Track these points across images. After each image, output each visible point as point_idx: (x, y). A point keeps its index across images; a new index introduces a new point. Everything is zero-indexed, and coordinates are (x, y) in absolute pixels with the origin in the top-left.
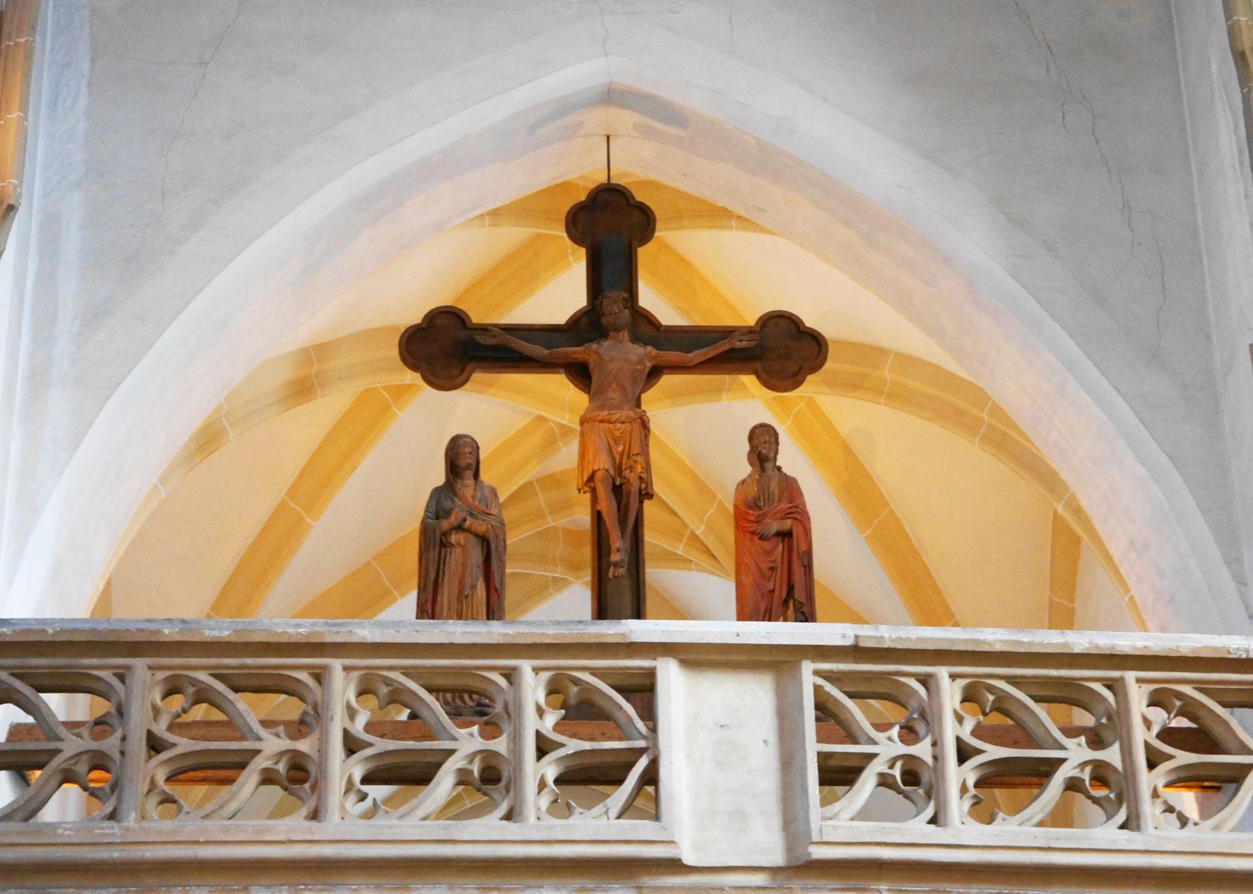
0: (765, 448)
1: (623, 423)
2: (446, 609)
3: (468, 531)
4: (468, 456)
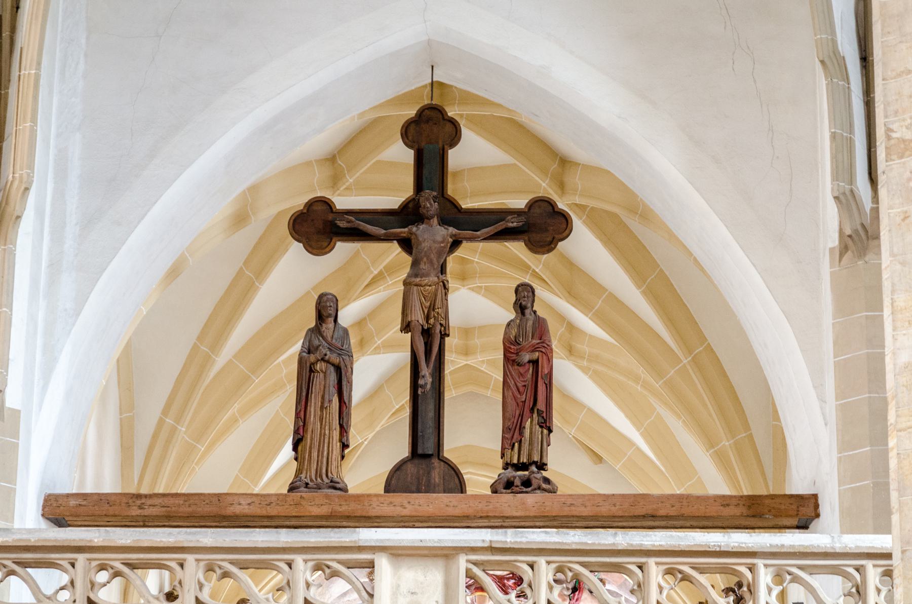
0: (524, 301)
1: (430, 286)
2: (312, 416)
3: (328, 362)
4: (329, 308)
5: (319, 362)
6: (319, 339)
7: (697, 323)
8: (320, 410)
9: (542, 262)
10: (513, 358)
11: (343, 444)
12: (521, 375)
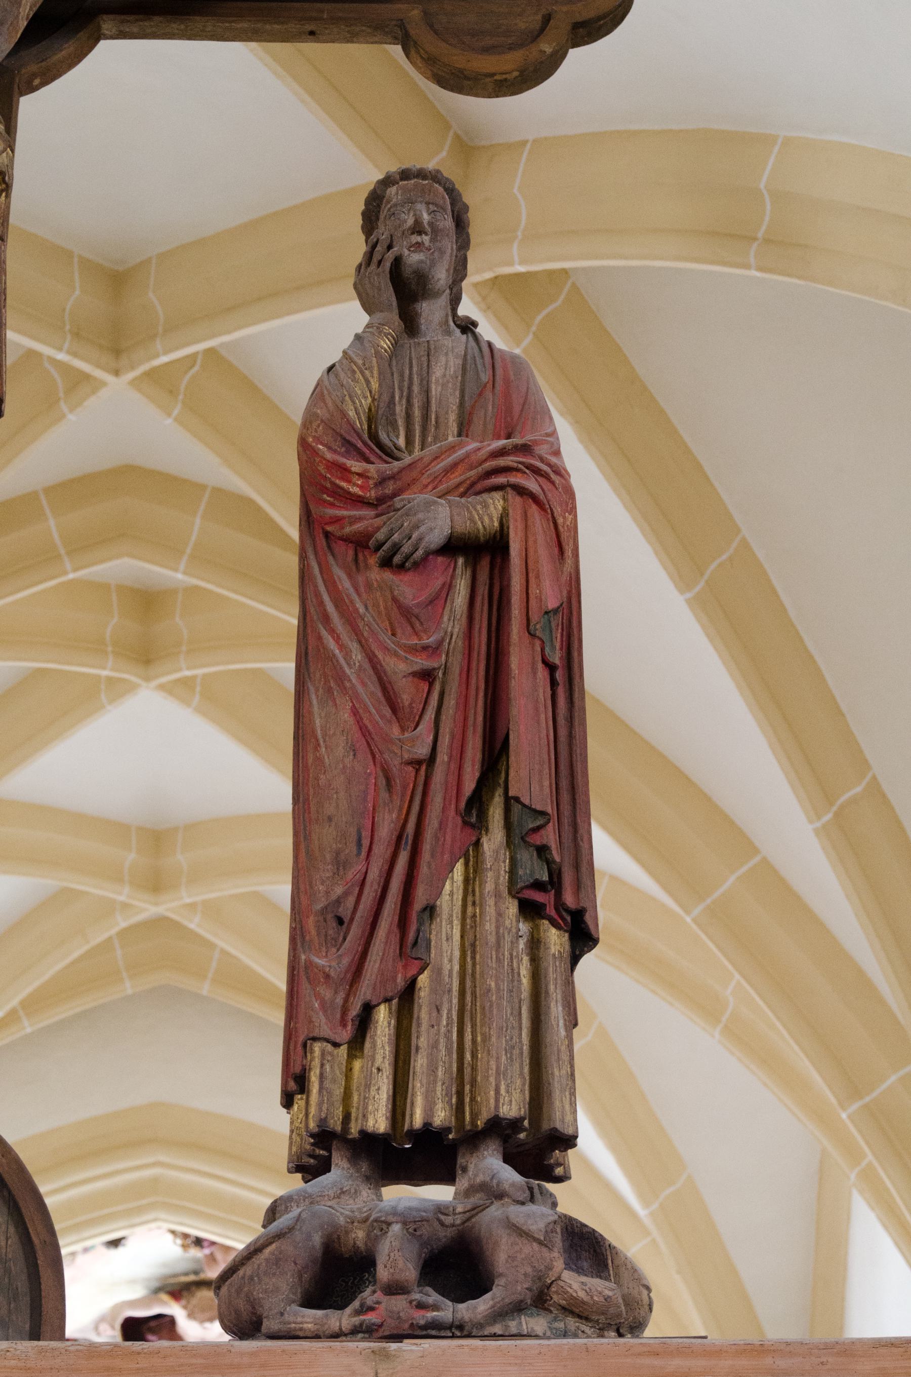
0: (418, 246)
7: (843, 715)
10: (358, 526)
12: (406, 613)
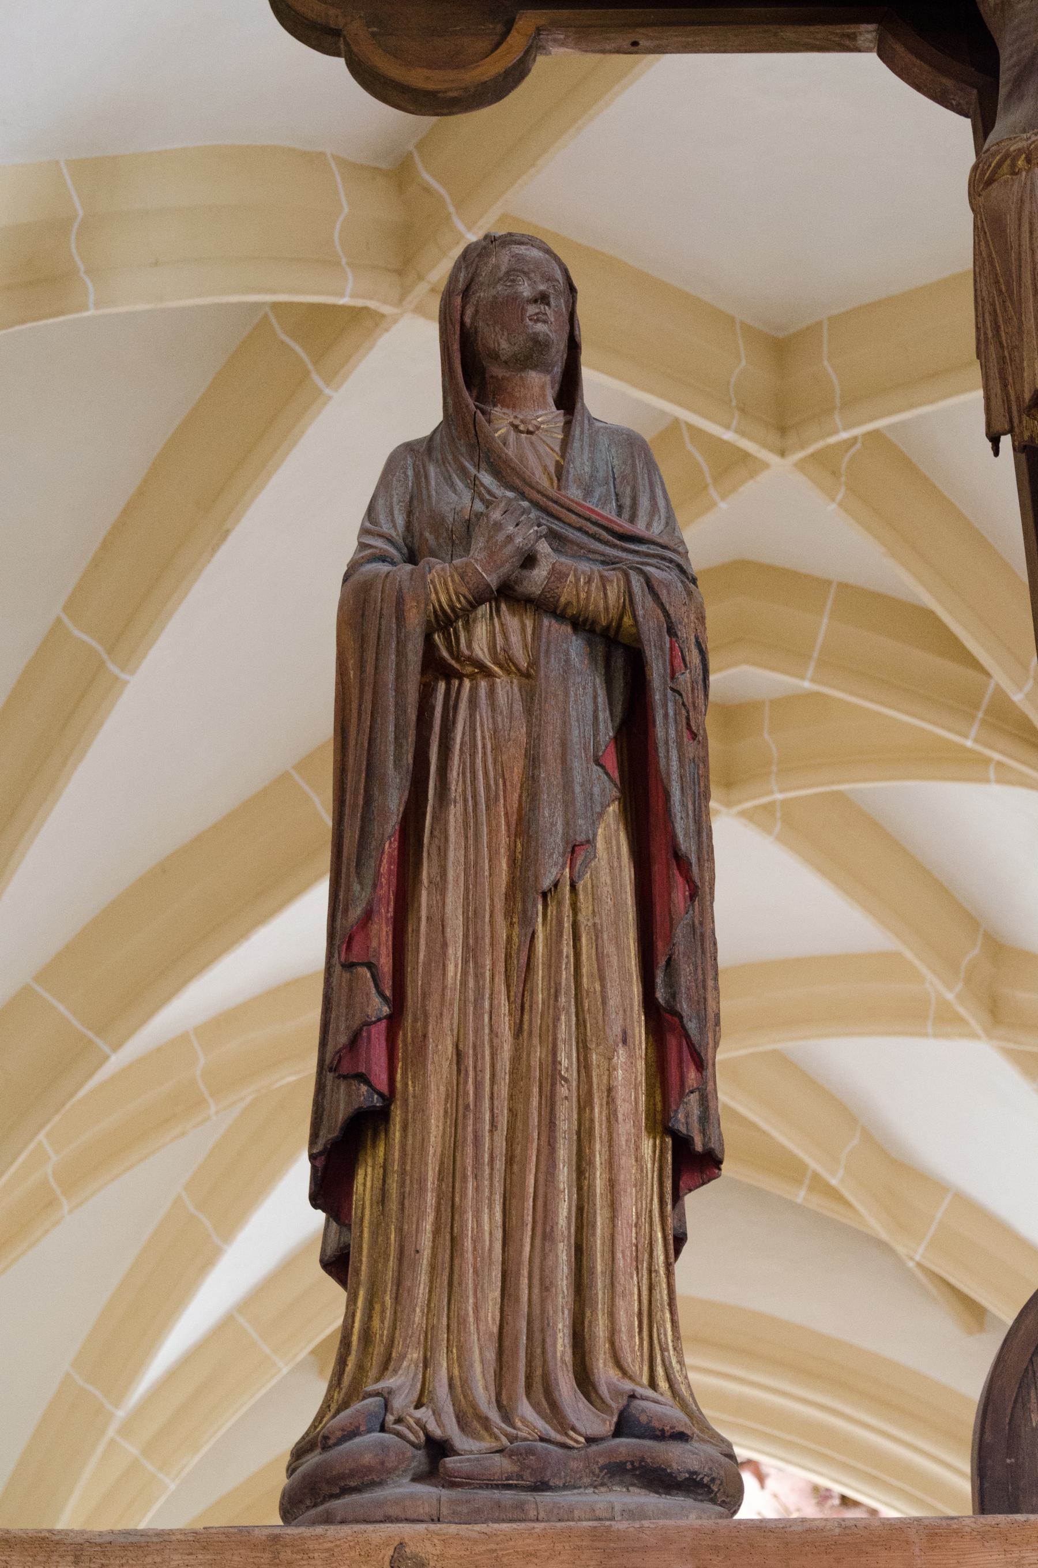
2: (455, 952)
4: (532, 309)
5: (484, 609)
6: (474, 484)
8: (509, 914)
9: (1032, 673)
11: (681, 1145)
